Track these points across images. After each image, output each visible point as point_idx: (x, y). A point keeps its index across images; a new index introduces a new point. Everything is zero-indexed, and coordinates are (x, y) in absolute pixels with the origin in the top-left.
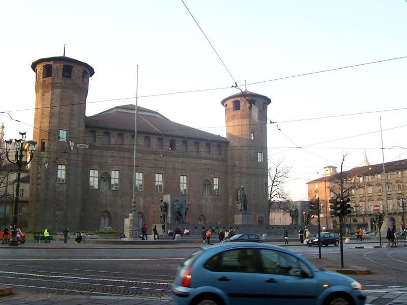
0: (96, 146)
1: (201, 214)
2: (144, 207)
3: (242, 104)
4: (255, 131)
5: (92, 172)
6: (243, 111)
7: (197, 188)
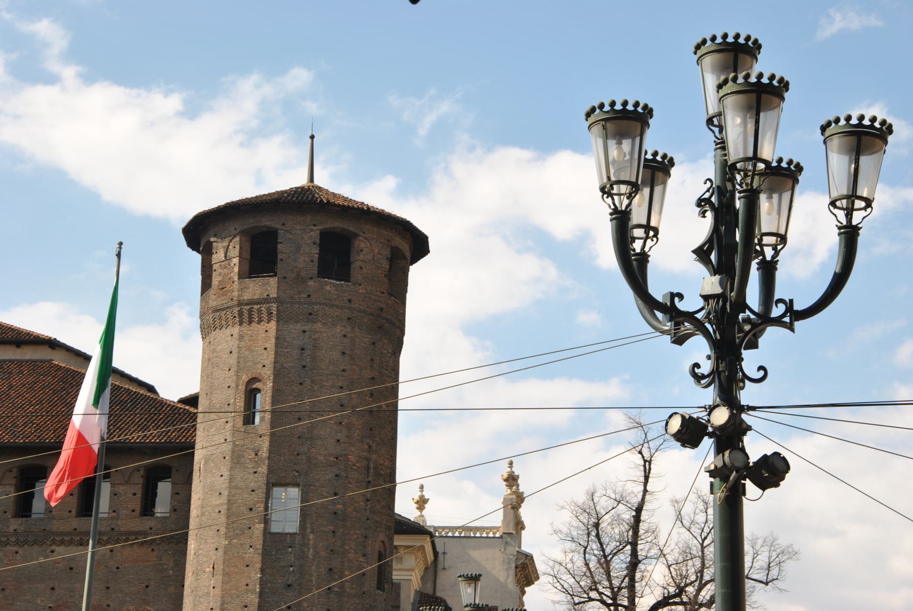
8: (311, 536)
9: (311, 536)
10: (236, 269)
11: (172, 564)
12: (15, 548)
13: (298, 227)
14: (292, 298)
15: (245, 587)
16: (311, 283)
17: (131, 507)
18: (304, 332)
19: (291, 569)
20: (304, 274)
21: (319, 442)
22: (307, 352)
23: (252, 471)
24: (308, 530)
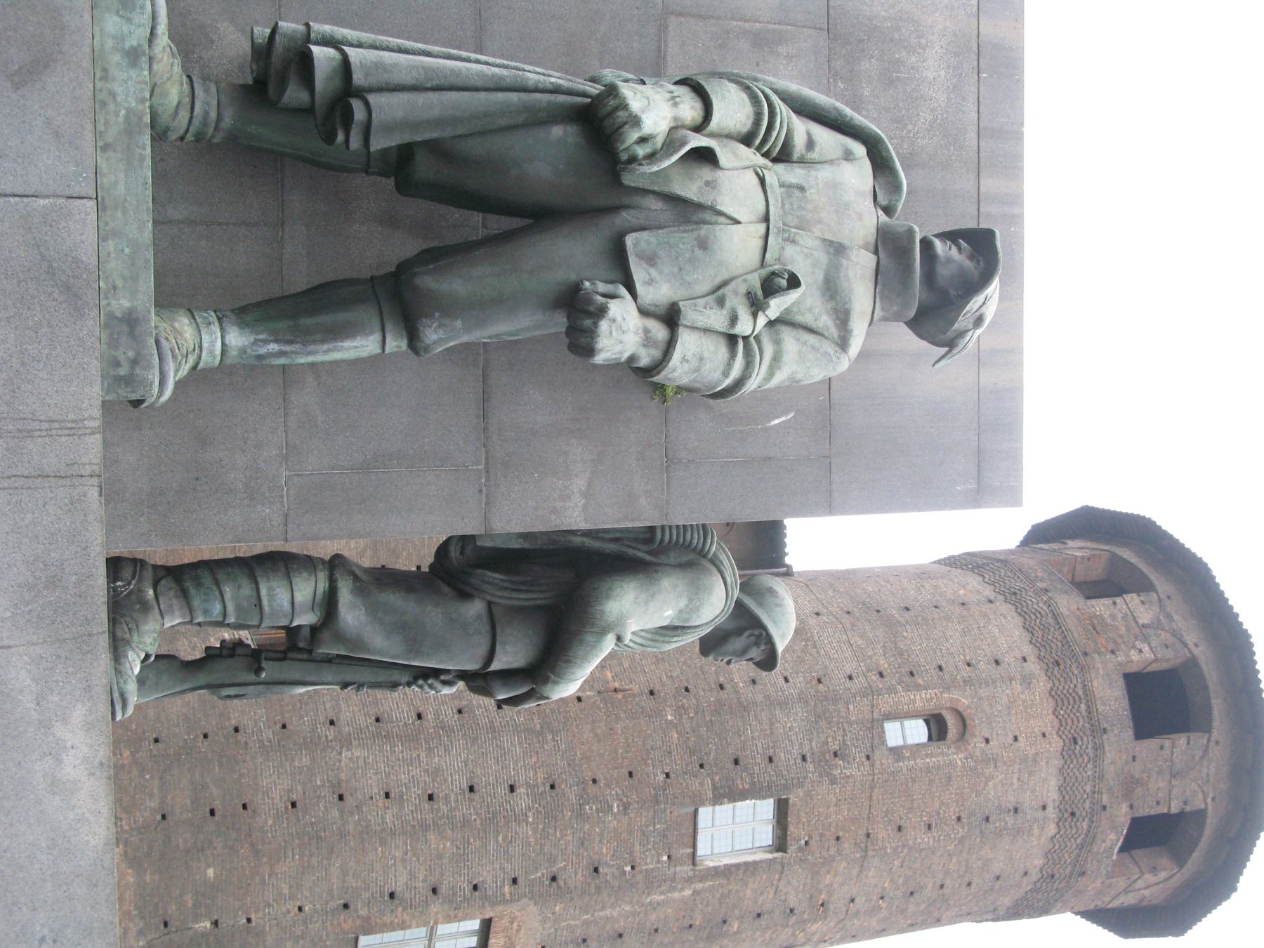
6: (1094, 626)
8: (688, 892)
9: (688, 892)
13: (1213, 769)
14: (1102, 777)
15: (588, 776)
16: (1124, 807)
18: (1044, 808)
19: (628, 868)
20: (1139, 791)
21: (855, 872)
22: (1010, 820)
23: (806, 750)
24: (699, 886)
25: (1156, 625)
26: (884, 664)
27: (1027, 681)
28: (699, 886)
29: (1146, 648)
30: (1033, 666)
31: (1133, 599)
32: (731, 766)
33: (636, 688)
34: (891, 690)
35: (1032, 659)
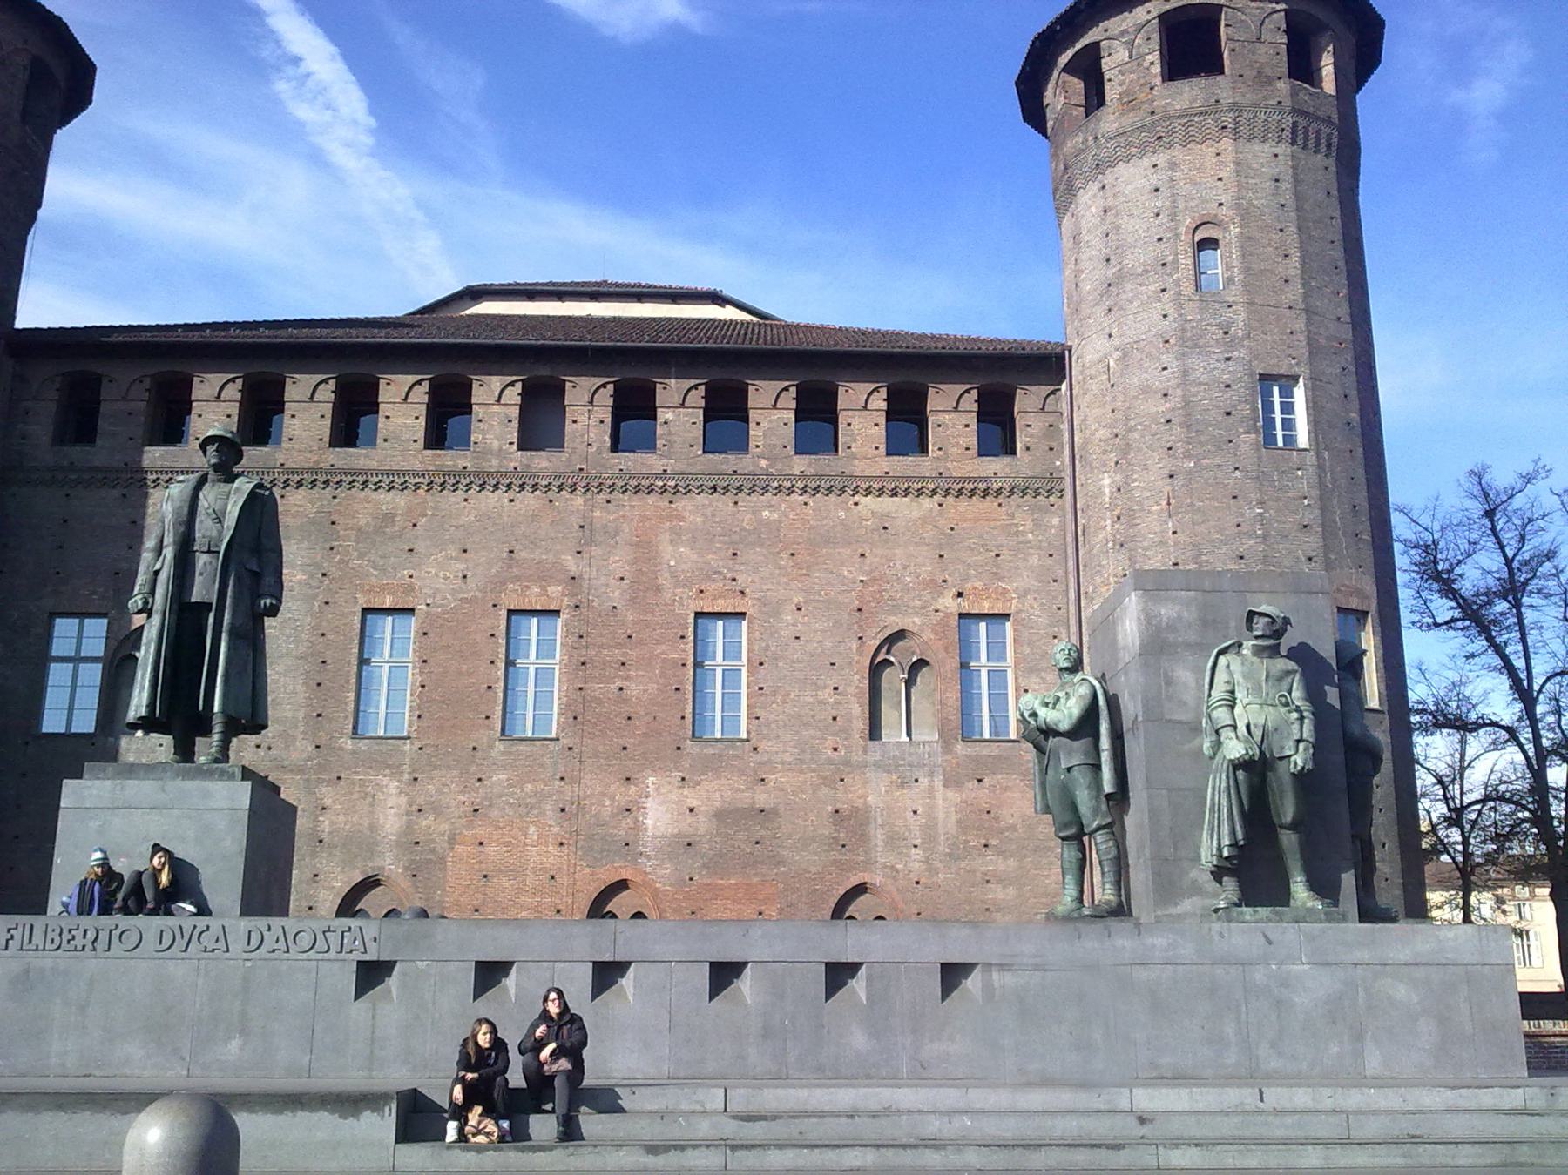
0: (97, 469)
1: (855, 881)
2: (411, 842)
3: (1112, 62)
4: (1216, 224)
5: (64, 628)
7: (827, 695)
10: (1157, 69)
11: (1029, 525)
12: (805, 498)
14: (1255, 105)
16: (1281, 85)
17: (963, 443)
20: (1268, 71)
23: (1222, 357)
25: (1131, 45)
26: (1155, 287)
27: (1173, 166)
28: (1322, 446)
29: (1149, 58)
30: (1162, 158)
31: (1106, 63)
32: (1230, 419)
33: (1168, 488)
34: (1177, 283)
35: (1154, 160)
